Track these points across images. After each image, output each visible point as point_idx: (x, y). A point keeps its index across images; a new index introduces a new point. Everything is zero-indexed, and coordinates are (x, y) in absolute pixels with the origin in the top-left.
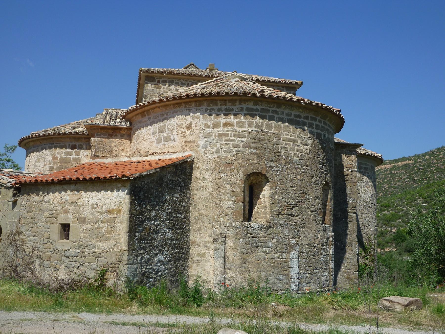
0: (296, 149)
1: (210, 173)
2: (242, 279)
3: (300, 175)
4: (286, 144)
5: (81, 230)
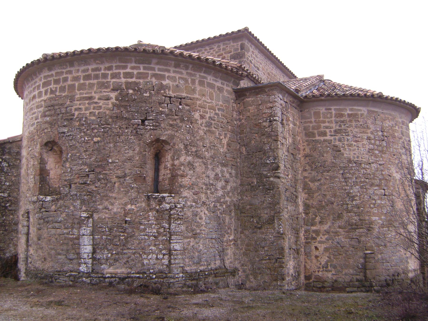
0: (92, 107)
3: (99, 136)
4: (80, 104)
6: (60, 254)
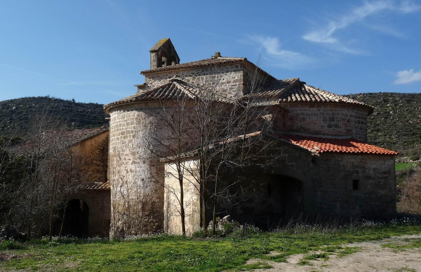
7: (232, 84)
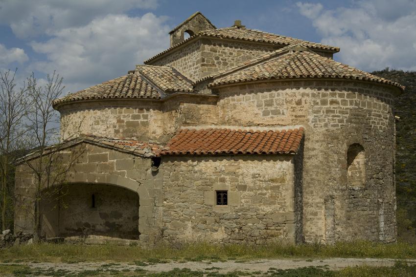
1: (319, 144)
2: (347, 233)
5: (242, 196)
6: (367, 230)
7: (195, 66)
